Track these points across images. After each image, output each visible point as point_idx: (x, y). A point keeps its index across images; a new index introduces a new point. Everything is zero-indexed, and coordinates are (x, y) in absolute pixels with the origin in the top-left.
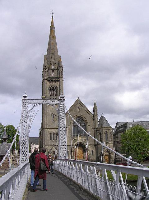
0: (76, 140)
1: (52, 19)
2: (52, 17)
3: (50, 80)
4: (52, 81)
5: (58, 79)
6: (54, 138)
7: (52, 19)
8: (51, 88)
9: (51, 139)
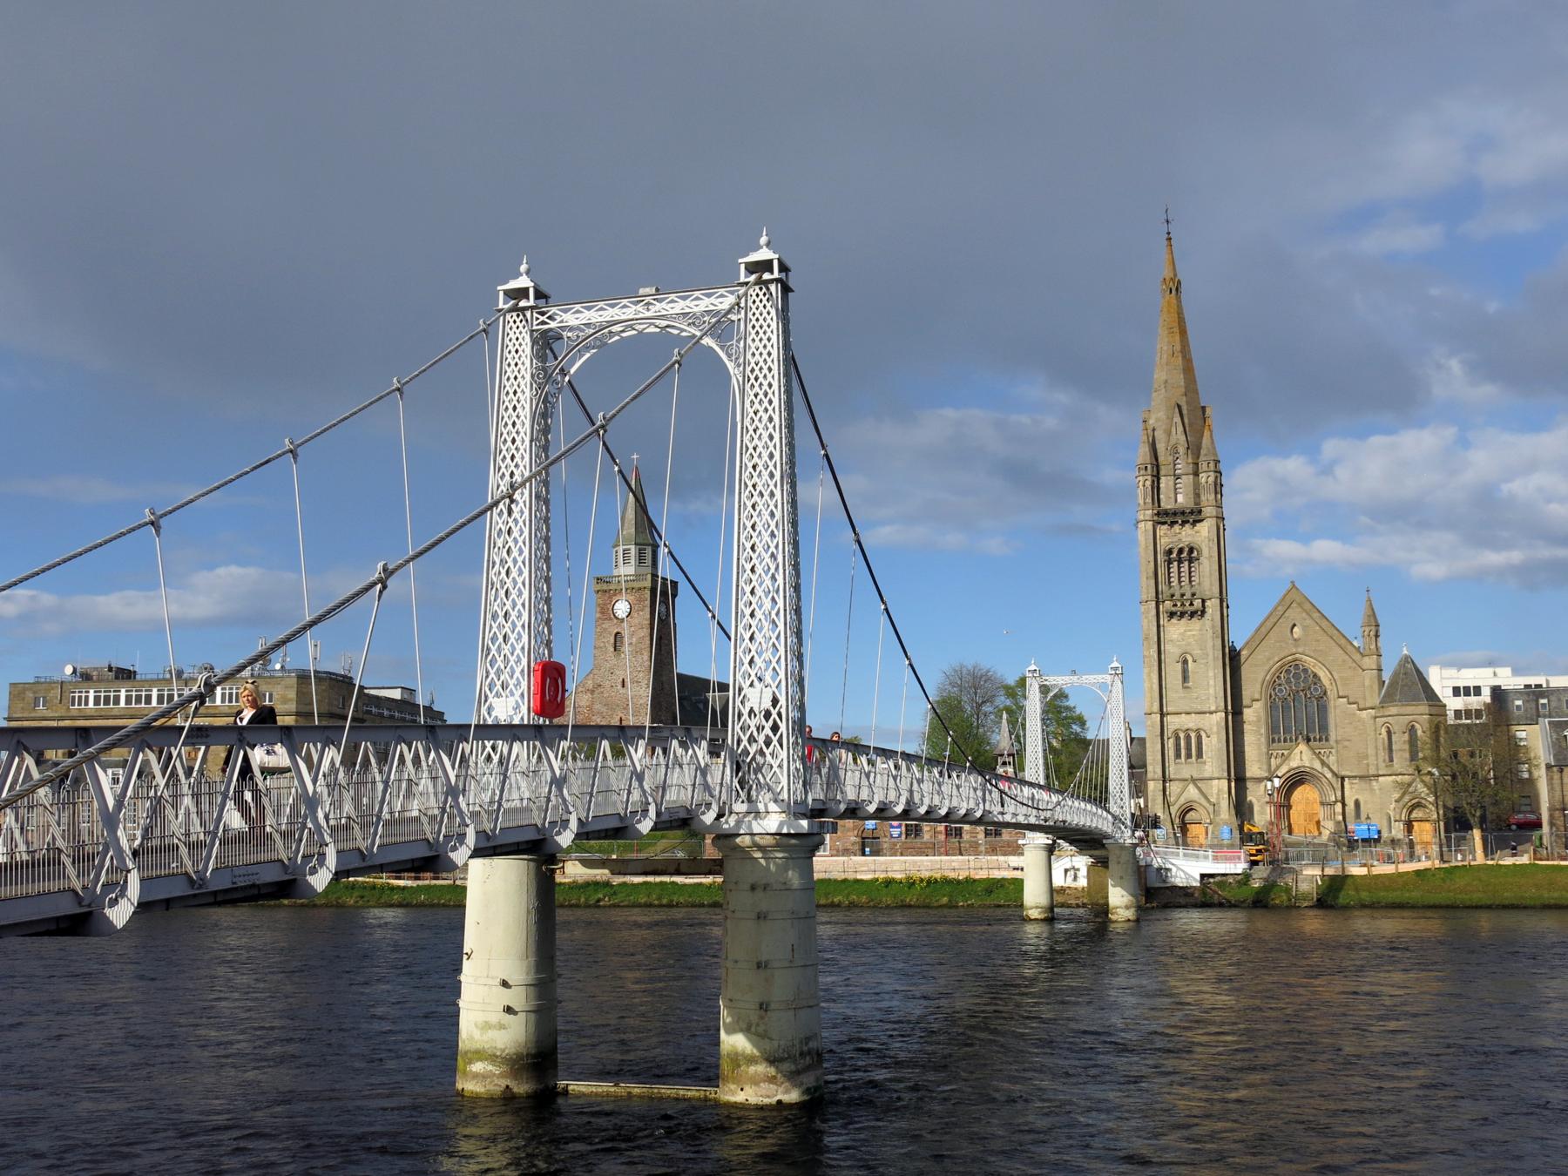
0: (1285, 758)
4: (1173, 523)
5: (1200, 512)
8: (1170, 552)
9: (1178, 756)
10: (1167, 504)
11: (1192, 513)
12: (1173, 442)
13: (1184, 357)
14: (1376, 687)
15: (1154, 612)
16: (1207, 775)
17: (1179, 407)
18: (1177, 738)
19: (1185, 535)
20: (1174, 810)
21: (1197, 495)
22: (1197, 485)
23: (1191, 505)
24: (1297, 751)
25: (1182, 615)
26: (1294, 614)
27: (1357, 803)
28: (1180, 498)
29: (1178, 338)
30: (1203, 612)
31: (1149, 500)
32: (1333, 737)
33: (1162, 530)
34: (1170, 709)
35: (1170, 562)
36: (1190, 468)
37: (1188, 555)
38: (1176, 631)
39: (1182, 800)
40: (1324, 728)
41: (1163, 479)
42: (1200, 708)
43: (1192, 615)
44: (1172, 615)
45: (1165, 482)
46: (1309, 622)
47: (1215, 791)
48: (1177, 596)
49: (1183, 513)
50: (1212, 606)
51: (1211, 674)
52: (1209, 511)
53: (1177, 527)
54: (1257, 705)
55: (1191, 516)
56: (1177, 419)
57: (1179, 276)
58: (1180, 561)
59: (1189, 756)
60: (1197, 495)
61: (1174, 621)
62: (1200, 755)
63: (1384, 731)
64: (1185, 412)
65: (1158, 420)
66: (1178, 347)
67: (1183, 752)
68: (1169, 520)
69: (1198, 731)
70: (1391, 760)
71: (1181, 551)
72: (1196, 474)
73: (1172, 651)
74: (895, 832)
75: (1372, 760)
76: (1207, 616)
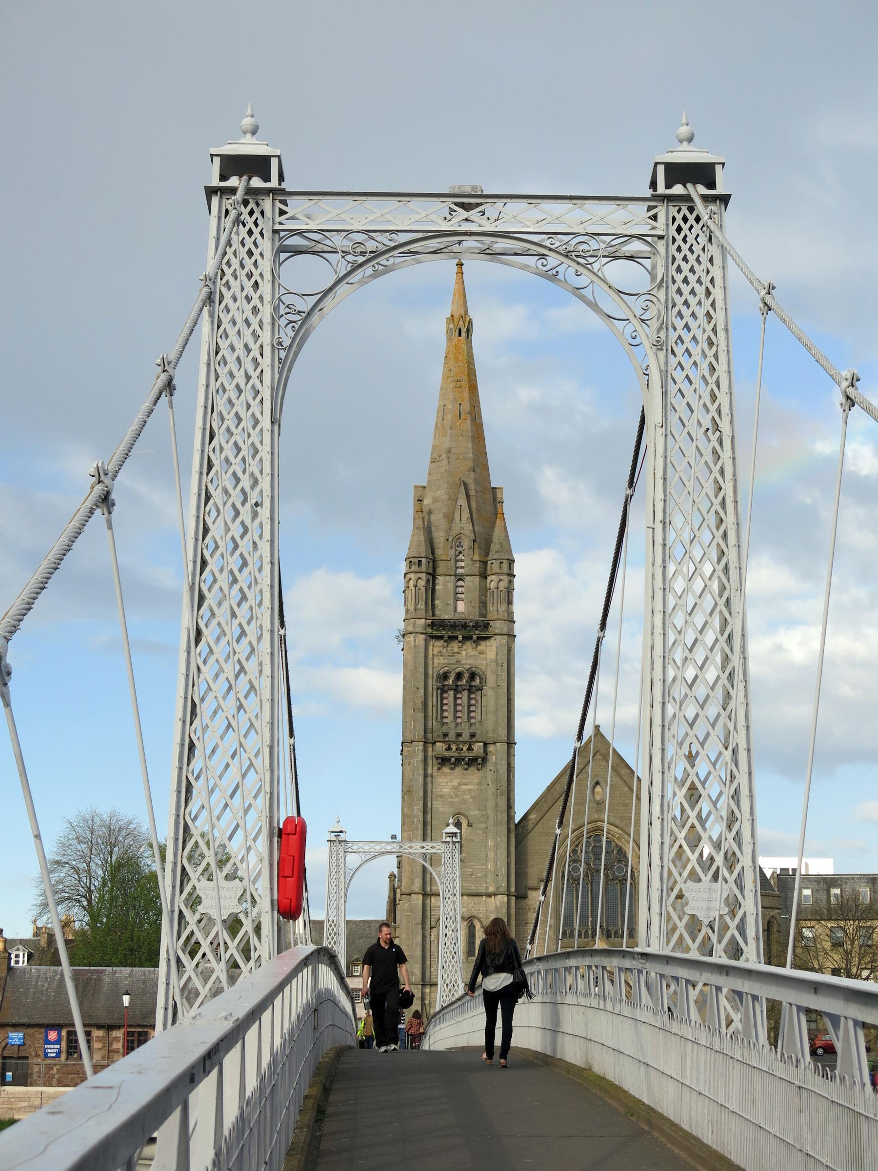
3: (442, 630)
4: (452, 638)
5: (486, 626)
8: (445, 676)
10: (444, 613)
11: (476, 626)
12: (455, 530)
13: (474, 420)
15: (421, 756)
17: (466, 485)
19: (467, 656)
21: (483, 604)
22: (484, 590)
23: (475, 616)
25: (458, 761)
28: (461, 606)
29: (466, 394)
30: (485, 760)
31: (421, 606)
33: (437, 646)
35: (443, 690)
36: (476, 568)
37: (468, 682)
38: (448, 782)
41: (440, 580)
43: (472, 762)
44: (444, 761)
45: (443, 584)
48: (452, 737)
49: (465, 626)
50: (497, 752)
51: (491, 843)
52: (497, 626)
53: (455, 645)
55: (475, 631)
56: (462, 501)
57: (472, 314)
58: (457, 690)
60: (483, 604)
61: (446, 770)
64: (472, 493)
65: (435, 500)
66: (466, 407)
68: (445, 634)
71: (459, 676)
72: (484, 576)
74: (52, 1050)
76: (490, 766)
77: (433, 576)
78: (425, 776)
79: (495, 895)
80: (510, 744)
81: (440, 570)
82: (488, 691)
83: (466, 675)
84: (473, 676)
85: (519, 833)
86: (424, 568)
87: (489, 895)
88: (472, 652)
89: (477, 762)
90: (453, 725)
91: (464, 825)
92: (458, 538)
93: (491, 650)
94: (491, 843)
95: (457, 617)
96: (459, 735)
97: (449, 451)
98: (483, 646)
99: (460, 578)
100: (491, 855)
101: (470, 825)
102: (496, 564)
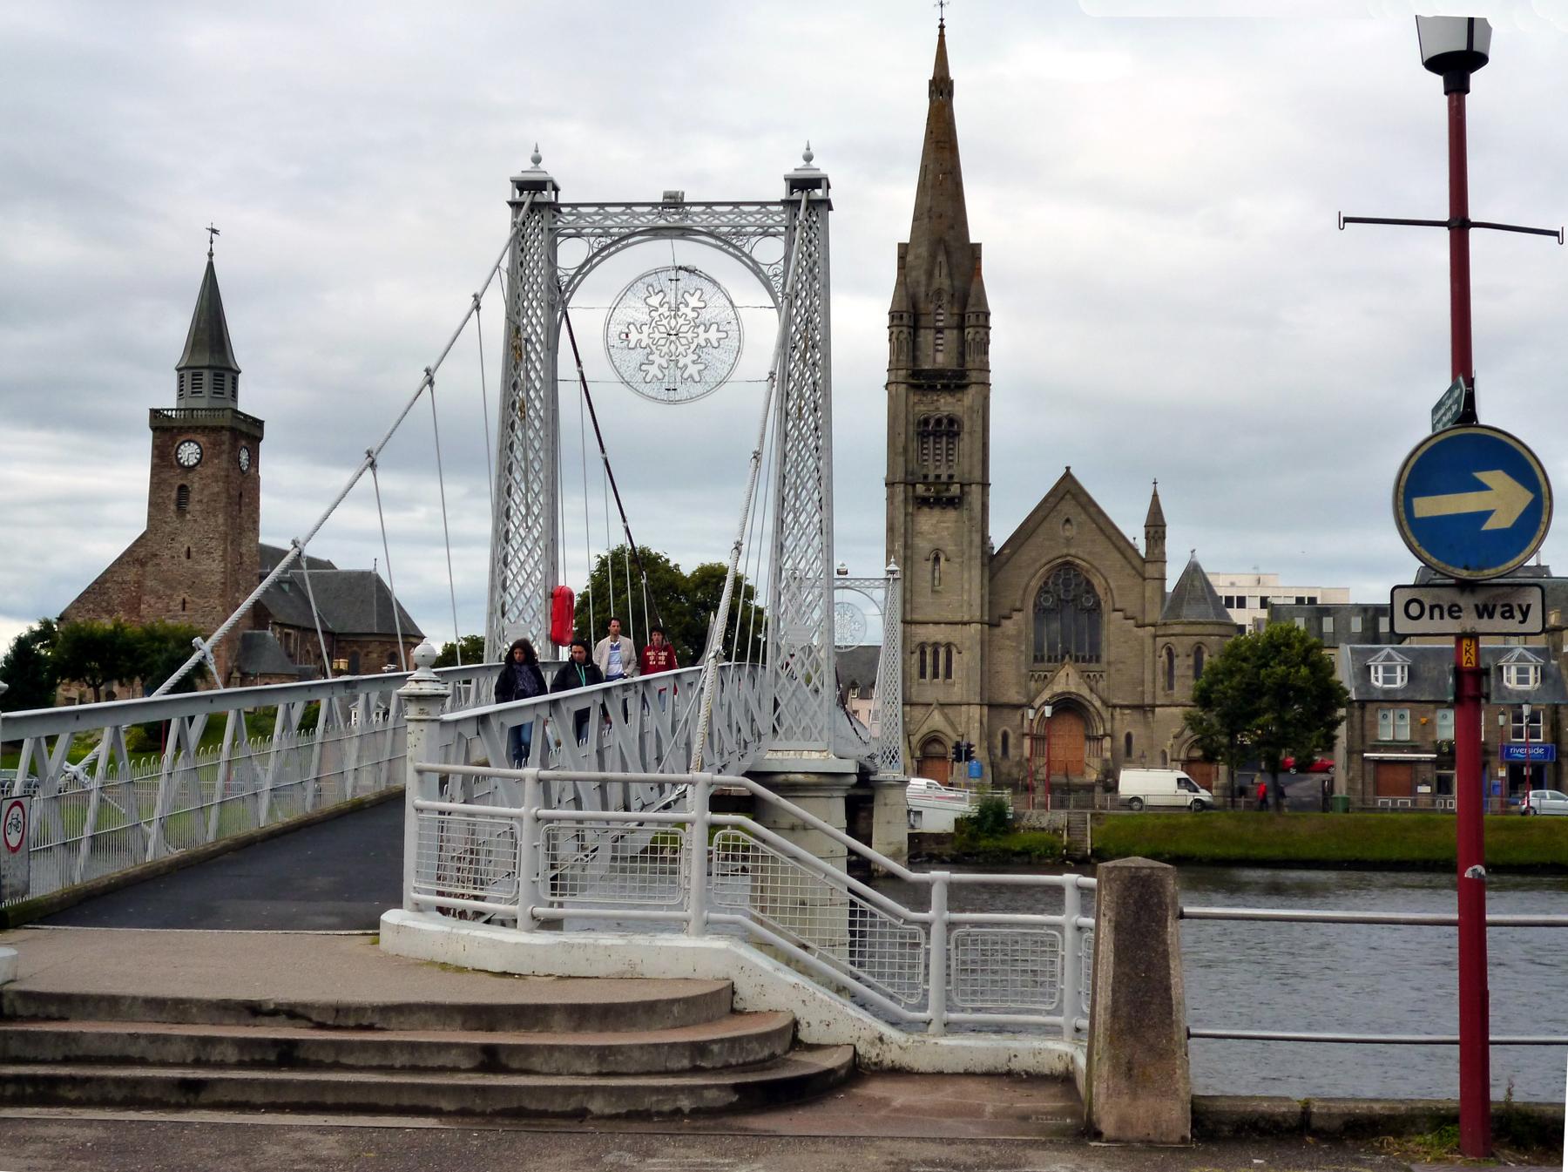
0: (1046, 680)
1: (942, 36)
2: (942, 27)
4: (932, 388)
6: (936, 666)
7: (942, 36)
8: (926, 422)
9: (923, 675)
12: (936, 285)
14: (1158, 599)
16: (955, 699)
18: (923, 653)
19: (946, 405)
20: (915, 739)
21: (962, 355)
22: (962, 342)
24: (1062, 673)
26: (1068, 508)
27: (1129, 737)
28: (940, 357)
32: (1104, 658)
34: (917, 617)
37: (947, 429)
39: (924, 730)
40: (1095, 646)
42: (951, 618)
44: (923, 502)
45: (927, 337)
46: (1084, 517)
47: (964, 718)
48: (931, 479)
52: (974, 376)
54: (1017, 616)
56: (941, 258)
59: (936, 675)
60: (962, 355)
62: (948, 675)
63: (1164, 652)
67: (929, 670)
69: (948, 646)
70: (1171, 687)
72: (961, 328)
73: (924, 545)
75: (1148, 687)
77: (915, 328)
78: (906, 515)
79: (969, 623)
80: (985, 485)
81: (924, 321)
82: (965, 436)
83: (945, 421)
84: (951, 421)
85: (993, 563)
86: (905, 321)
87: (965, 624)
88: (949, 399)
89: (953, 503)
90: (932, 467)
91: (942, 559)
92: (939, 292)
93: (970, 397)
94: (966, 576)
95: (937, 366)
96: (938, 477)
97: (930, 210)
98: (959, 395)
99: (940, 330)
100: (966, 586)
101: (947, 560)
102: (973, 317)
